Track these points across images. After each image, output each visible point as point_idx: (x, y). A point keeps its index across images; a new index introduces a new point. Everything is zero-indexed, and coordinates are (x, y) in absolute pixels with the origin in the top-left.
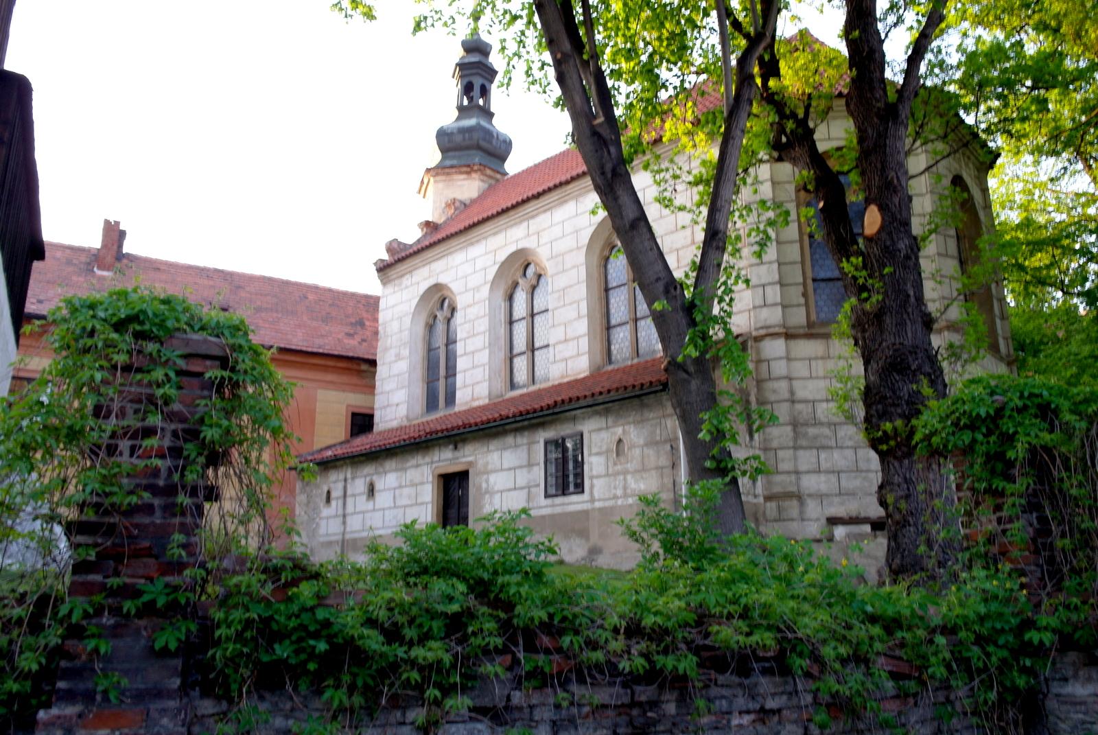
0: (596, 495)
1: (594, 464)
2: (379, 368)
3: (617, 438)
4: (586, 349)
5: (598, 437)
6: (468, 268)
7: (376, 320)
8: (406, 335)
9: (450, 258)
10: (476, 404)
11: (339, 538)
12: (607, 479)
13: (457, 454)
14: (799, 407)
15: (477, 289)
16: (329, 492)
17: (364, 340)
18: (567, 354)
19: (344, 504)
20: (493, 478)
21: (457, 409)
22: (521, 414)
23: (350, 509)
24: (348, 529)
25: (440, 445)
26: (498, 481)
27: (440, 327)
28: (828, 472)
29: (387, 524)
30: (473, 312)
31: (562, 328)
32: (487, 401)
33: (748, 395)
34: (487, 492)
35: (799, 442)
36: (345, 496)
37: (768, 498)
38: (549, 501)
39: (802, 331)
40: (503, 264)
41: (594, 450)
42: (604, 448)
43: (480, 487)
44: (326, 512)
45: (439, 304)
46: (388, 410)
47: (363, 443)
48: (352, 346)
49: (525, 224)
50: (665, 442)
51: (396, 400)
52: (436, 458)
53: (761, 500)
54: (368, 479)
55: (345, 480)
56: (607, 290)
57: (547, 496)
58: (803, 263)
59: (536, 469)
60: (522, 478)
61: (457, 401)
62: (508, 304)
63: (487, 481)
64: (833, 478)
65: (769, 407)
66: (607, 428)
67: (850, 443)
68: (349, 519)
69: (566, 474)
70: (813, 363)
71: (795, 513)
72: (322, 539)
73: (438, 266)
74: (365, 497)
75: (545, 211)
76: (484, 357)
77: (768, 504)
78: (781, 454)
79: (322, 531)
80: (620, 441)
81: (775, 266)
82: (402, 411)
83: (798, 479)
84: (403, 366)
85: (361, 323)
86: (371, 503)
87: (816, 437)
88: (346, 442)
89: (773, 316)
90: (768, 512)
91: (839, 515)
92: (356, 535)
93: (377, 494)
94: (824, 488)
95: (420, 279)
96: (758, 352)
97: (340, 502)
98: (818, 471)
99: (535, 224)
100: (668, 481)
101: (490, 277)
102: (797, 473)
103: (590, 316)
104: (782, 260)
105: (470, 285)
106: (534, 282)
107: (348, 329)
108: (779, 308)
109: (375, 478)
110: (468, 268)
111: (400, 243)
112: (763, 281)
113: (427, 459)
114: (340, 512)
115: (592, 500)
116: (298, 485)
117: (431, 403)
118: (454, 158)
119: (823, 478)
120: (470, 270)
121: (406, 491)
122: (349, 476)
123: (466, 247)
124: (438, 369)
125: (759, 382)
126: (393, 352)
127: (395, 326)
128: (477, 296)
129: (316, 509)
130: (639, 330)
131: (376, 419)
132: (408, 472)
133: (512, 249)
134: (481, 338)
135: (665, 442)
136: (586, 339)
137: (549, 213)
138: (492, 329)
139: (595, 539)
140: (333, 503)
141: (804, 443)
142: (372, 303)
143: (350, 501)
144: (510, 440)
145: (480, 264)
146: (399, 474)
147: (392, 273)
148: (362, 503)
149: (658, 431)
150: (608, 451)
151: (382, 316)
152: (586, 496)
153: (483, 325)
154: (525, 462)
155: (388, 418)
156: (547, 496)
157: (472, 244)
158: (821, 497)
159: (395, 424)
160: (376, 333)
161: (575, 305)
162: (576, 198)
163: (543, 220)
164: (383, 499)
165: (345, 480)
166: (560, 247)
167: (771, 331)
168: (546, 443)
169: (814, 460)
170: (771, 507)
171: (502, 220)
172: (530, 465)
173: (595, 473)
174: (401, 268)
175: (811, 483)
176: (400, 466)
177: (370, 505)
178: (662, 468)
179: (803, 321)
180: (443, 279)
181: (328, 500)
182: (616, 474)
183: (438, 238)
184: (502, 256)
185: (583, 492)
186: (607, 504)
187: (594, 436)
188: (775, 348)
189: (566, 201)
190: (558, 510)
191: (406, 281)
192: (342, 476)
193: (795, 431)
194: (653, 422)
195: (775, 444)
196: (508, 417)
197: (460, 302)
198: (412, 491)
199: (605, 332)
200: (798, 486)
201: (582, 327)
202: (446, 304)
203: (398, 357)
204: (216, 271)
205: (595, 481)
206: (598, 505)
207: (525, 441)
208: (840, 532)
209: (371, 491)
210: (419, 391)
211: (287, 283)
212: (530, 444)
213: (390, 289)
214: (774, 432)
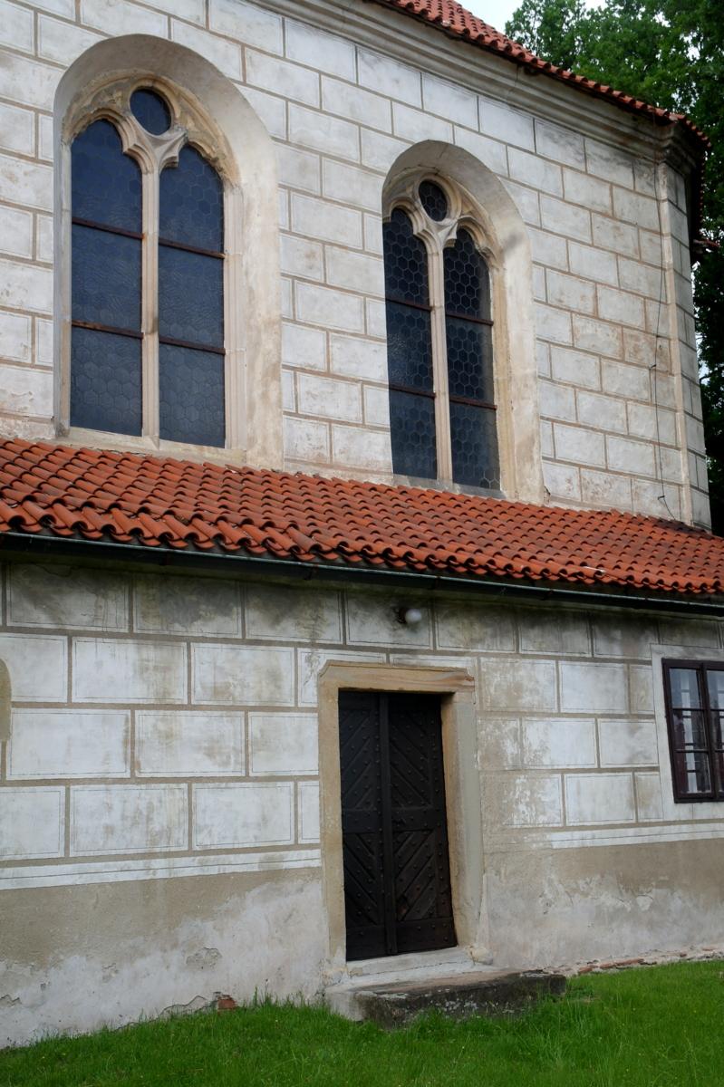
13: (406, 638)
18: (332, 412)
20: (534, 732)
25: (343, 597)
34: (517, 770)
38: (684, 810)
43: (496, 754)
52: (331, 634)
59: (647, 726)
60: (617, 744)
63: (518, 737)
113: (290, 629)
121: (192, 725)
132: (202, 653)
144: (577, 639)
146: (151, 653)
154: (620, 709)
156: (681, 796)
162: (359, 44)
168: (668, 665)
176: (152, 626)
198: (228, 729)
212: (632, 662)
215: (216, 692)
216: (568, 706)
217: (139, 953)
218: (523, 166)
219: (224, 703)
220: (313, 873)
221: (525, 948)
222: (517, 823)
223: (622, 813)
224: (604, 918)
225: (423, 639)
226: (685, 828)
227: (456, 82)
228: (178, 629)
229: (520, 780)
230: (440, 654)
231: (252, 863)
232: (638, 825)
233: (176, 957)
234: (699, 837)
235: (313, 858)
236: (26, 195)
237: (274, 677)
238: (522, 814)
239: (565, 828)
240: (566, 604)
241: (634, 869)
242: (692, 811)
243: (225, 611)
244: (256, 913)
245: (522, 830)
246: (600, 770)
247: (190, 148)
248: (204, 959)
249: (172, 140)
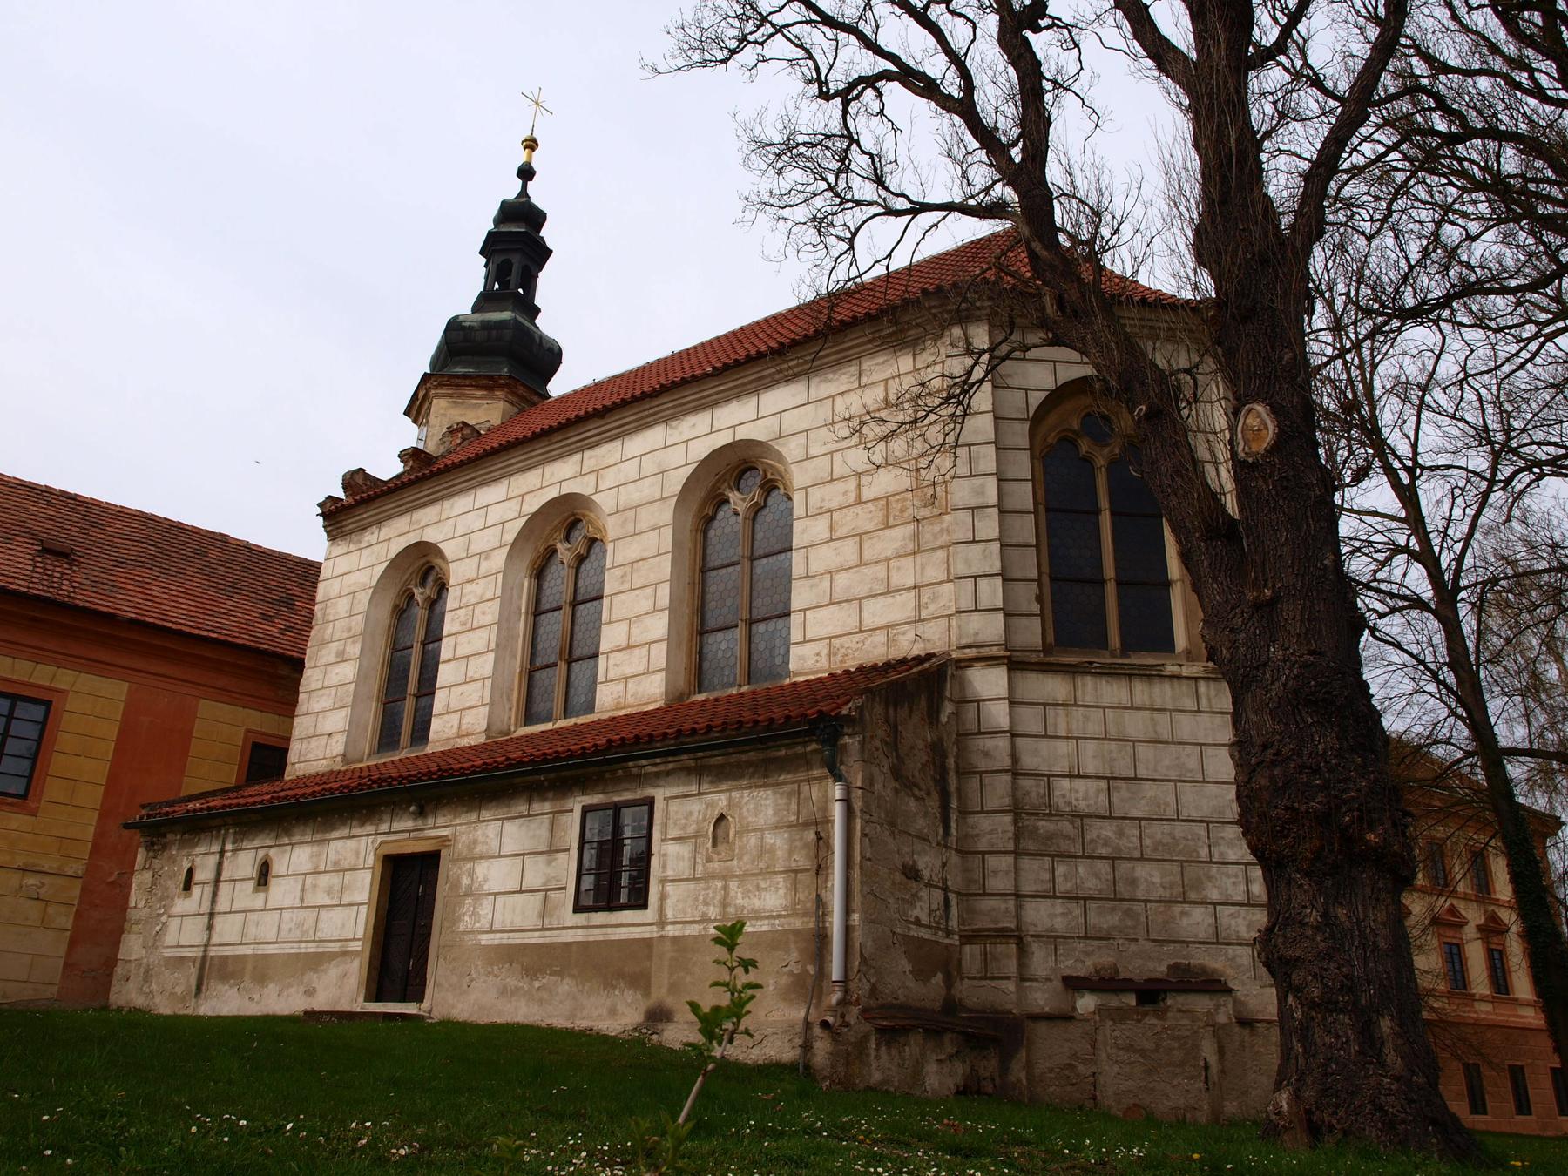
0: (670, 914)
1: (670, 858)
2: (307, 673)
3: (716, 814)
4: (662, 663)
5: (679, 812)
6: (474, 521)
7: (312, 601)
8: (358, 623)
9: (447, 504)
10: (464, 742)
11: (198, 952)
12: (692, 885)
14: (1026, 783)
15: (486, 554)
16: (190, 872)
17: (289, 629)
18: (628, 671)
19: (215, 894)
20: (481, 869)
21: (429, 749)
22: (545, 759)
23: (222, 905)
24: (215, 940)
26: (494, 875)
27: (419, 613)
28: (1069, 898)
29: (284, 935)
30: (474, 591)
31: (624, 626)
32: (482, 739)
33: (944, 756)
34: (467, 895)
35: (1023, 844)
36: (217, 881)
37: (969, 937)
38: (581, 918)
39: (1034, 658)
40: (534, 516)
41: (673, 833)
42: (691, 829)
43: (456, 885)
44: (182, 905)
45: (420, 579)
46: (314, 743)
47: (261, 793)
48: (268, 635)
49: (578, 456)
50: (806, 825)
51: (328, 726)
52: (384, 827)
53: (955, 940)
54: (261, 853)
55: (222, 853)
56: (704, 570)
57: (578, 908)
58: (1037, 546)
59: (562, 857)
61: (432, 736)
62: (534, 582)
63: (471, 874)
64: (1076, 909)
65: (975, 781)
66: (700, 794)
67: (1104, 851)
68: (218, 920)
69: (615, 876)
70: (1051, 711)
71: (1011, 967)
72: (168, 953)
73: (427, 514)
74: (251, 885)
75: (612, 439)
76: (486, 665)
77: (967, 948)
78: (992, 861)
79: (170, 939)
80: (722, 818)
81: (996, 547)
82: (337, 746)
83: (1019, 907)
84: (348, 671)
85: (289, 602)
86: (262, 895)
87: (1050, 837)
88: (237, 788)
89: (990, 628)
90: (966, 963)
91: (1081, 971)
92: (227, 951)
93: (273, 882)
94: (1060, 925)
95: (390, 538)
96: (962, 684)
97: (208, 889)
98: (1050, 895)
99: (593, 458)
100: (806, 896)
101: (510, 537)
102: (1018, 896)
103: (673, 609)
104: (1008, 541)
105: (474, 549)
106: (582, 550)
107: (266, 609)
108: (1000, 615)
109: (272, 852)
110: (474, 521)
111: (368, 477)
112: (974, 571)
113: (369, 829)
114: (206, 908)
115: (662, 923)
116: (141, 855)
117: (388, 736)
118: (469, 365)
119: (1059, 907)
120: (478, 529)
121: (324, 880)
122: (229, 846)
123: (474, 487)
124: (406, 677)
125: (963, 736)
126: (334, 647)
127: (342, 606)
129: (167, 900)
130: (756, 639)
131: (292, 756)
132: (335, 845)
133: (553, 493)
134: (484, 633)
135: (806, 825)
136: (664, 645)
137: (618, 443)
138: (504, 621)
139: (660, 993)
140: (196, 890)
141: (1031, 845)
142: (307, 572)
143: (224, 889)
144: (522, 808)
145: (495, 515)
146: (316, 848)
147: (350, 523)
149: (794, 806)
150: (698, 835)
151: (322, 591)
152: (649, 915)
153: (490, 613)
155: (311, 756)
156: (578, 908)
157: (485, 484)
158: (1053, 939)
159: (322, 766)
160: (310, 616)
161: (649, 590)
162: (666, 420)
163: (607, 453)
164: (282, 891)
165: (222, 853)
166: (631, 495)
167: (986, 652)
168: (586, 811)
169: (1047, 876)
170: (971, 953)
171: (541, 448)
172: (552, 851)
173: (670, 873)
174: (364, 515)
175: (1040, 915)
176: (318, 837)
177: (258, 901)
178: (796, 872)
179: (1037, 641)
180: (431, 536)
181: (187, 886)
182: (709, 877)
183: (426, 475)
184: (533, 504)
185: (644, 906)
186: (689, 930)
187: (674, 806)
188: (989, 683)
189: (649, 426)
190: (596, 935)
191: (370, 537)
192: (216, 848)
193: (1015, 822)
194: (786, 788)
195: (983, 844)
196: (521, 763)
197: (457, 573)
199: (696, 639)
200: (1018, 917)
201: (659, 626)
202: (431, 579)
203: (342, 658)
204: (63, 494)
205: (670, 888)
206: (671, 931)
207: (547, 807)
208: (1086, 1003)
209: (264, 875)
210: (371, 714)
211: (179, 527)
213: (341, 547)
214: (984, 823)
215: (336, 863)
216: (506, 850)
217: (290, 985)
218: (792, 421)
219: (339, 870)
220: (356, 953)
221: (453, 1007)
222: (462, 927)
223: (532, 920)
224: (504, 992)
225: (430, 821)
226: (580, 932)
227: (738, 397)
228: (328, 836)
229: (469, 900)
230: (444, 827)
231: (334, 947)
232: (543, 929)
233: (302, 989)
234: (591, 939)
235: (356, 946)
237: (357, 853)
238: (466, 922)
239: (491, 932)
240: (518, 780)
241: (535, 961)
242: (588, 919)
243: (344, 823)
244: (333, 971)
245: (465, 933)
246: (521, 892)
248: (310, 992)
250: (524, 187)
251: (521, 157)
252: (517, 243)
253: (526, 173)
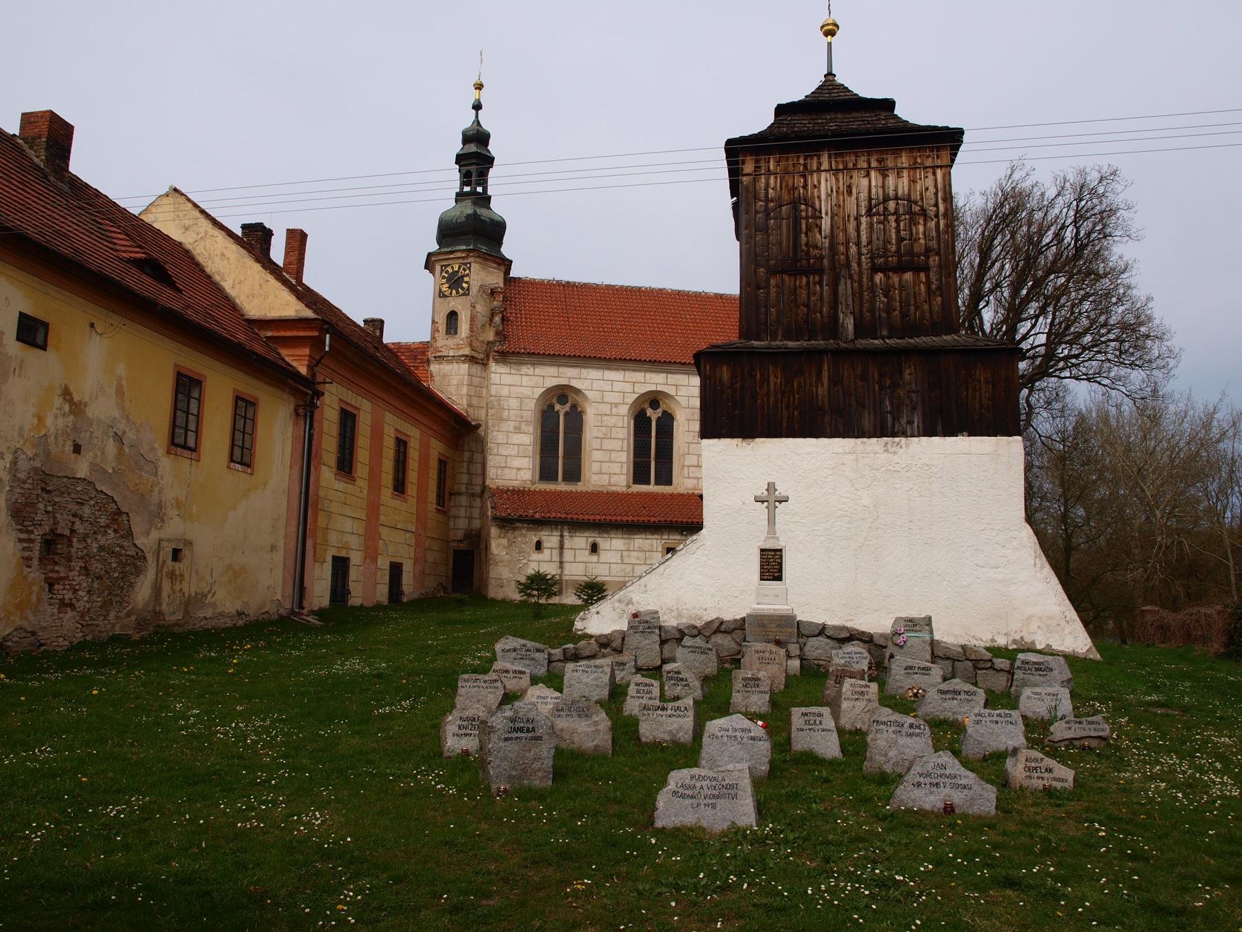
19: (561, 555)
24: (566, 572)
36: (562, 547)
54: (591, 540)
55: (562, 536)
68: (566, 565)
97: (556, 553)
114: (556, 558)
121: (634, 554)
122: (566, 534)
128: (615, 410)
140: (547, 552)
148: (585, 555)
164: (604, 556)
165: (562, 536)
177: (594, 558)
191: (525, 369)
198: (642, 555)
203: (518, 430)
219: (641, 550)
236: (621, 436)
247: (664, 412)
249: (659, 412)
250: (477, 116)
251: (475, 94)
252: (475, 158)
253: (477, 107)
